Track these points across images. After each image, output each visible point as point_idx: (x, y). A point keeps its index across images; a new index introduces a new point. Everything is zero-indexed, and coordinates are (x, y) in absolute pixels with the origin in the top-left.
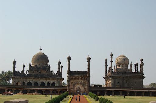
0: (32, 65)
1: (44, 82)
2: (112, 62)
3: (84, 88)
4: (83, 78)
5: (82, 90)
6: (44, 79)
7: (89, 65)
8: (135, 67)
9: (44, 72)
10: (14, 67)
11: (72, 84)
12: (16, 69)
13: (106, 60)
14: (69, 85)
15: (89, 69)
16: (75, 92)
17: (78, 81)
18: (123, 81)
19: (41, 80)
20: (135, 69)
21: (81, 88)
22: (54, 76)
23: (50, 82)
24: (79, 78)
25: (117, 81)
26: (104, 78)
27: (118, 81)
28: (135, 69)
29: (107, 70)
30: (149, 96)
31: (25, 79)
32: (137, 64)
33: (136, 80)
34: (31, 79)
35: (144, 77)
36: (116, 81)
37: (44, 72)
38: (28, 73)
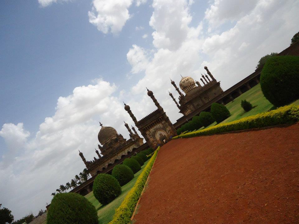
0: (102, 146)
1: (124, 154)
2: (177, 89)
4: (158, 120)
5: (166, 135)
6: (122, 151)
7: (155, 101)
8: (202, 81)
13: (171, 95)
14: (147, 140)
15: (157, 104)
16: (160, 142)
17: (155, 127)
18: (202, 100)
20: (204, 83)
21: (164, 133)
24: (153, 123)
28: (204, 83)
29: (178, 103)
30: (248, 89)
32: (203, 76)
33: (214, 91)
34: (108, 160)
35: (219, 84)
36: (195, 105)
37: (117, 145)
38: (102, 156)
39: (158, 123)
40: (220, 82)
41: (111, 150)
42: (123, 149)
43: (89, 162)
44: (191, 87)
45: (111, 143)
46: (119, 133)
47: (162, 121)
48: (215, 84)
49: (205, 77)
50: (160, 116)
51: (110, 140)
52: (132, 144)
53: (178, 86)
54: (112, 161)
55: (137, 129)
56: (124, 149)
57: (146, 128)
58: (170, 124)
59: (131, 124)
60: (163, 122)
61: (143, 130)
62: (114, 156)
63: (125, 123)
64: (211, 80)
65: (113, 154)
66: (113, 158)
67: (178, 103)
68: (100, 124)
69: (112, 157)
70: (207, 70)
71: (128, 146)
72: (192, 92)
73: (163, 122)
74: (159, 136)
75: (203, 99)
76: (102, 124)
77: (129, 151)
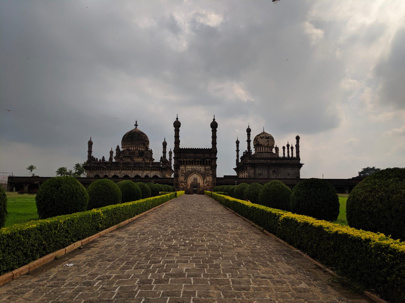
1: (140, 175)
2: (249, 141)
3: (205, 181)
4: (204, 162)
5: (201, 184)
6: (140, 170)
7: (214, 137)
8: (284, 151)
9: (140, 160)
10: (90, 152)
11: (183, 173)
12: (94, 154)
13: (238, 142)
14: (176, 176)
15: (214, 143)
17: (195, 167)
18: (268, 172)
19: (134, 172)
20: (284, 154)
21: (200, 181)
22: (156, 167)
23: (149, 175)
24: (195, 161)
25: (258, 171)
26: (235, 169)
27: (260, 172)
28: (284, 154)
29: (240, 157)
31: (108, 169)
32: (288, 146)
33: (290, 171)
34: (117, 170)
36: (257, 172)
37: (140, 160)
38: (114, 160)
39: (201, 165)
40: (303, 165)
41: (129, 160)
42: (143, 168)
43: (95, 158)
44: (266, 148)
45: (134, 153)
46: (150, 147)
47: (207, 165)
48: (295, 163)
49: (290, 147)
50: (209, 158)
51: (135, 149)
52: (157, 170)
53: (252, 139)
54: (121, 174)
55: (173, 155)
56: (144, 169)
57: (184, 161)
58: (214, 175)
59: (171, 146)
60: (208, 167)
61: (179, 161)
62: (128, 170)
63: (165, 140)
64: (295, 155)
65: (127, 166)
66: (123, 172)
67: (240, 157)
68: (136, 123)
69: (124, 170)
70: (298, 142)
71: (151, 169)
72: (265, 155)
73: (207, 167)
74: (192, 180)
75: (271, 172)
76: (138, 125)
77: (148, 175)
